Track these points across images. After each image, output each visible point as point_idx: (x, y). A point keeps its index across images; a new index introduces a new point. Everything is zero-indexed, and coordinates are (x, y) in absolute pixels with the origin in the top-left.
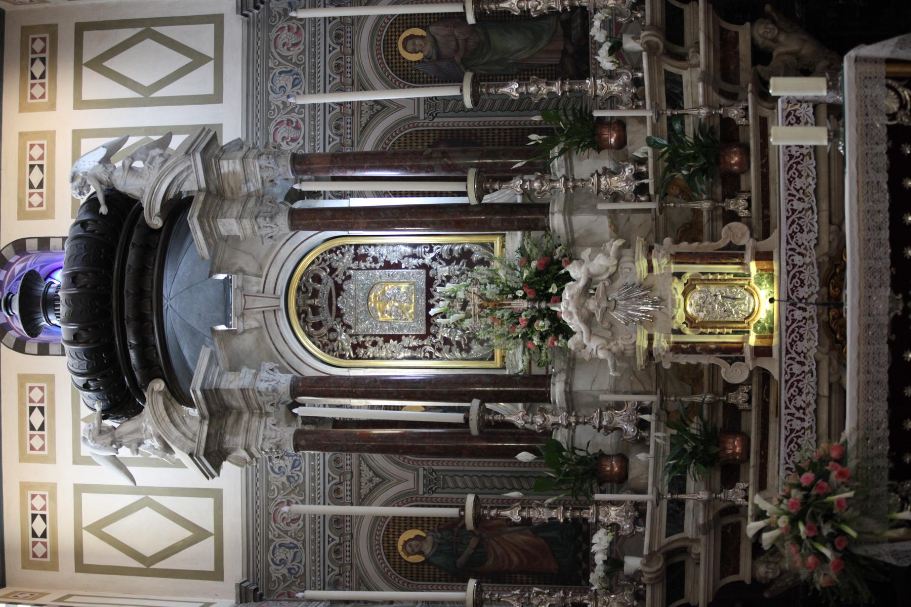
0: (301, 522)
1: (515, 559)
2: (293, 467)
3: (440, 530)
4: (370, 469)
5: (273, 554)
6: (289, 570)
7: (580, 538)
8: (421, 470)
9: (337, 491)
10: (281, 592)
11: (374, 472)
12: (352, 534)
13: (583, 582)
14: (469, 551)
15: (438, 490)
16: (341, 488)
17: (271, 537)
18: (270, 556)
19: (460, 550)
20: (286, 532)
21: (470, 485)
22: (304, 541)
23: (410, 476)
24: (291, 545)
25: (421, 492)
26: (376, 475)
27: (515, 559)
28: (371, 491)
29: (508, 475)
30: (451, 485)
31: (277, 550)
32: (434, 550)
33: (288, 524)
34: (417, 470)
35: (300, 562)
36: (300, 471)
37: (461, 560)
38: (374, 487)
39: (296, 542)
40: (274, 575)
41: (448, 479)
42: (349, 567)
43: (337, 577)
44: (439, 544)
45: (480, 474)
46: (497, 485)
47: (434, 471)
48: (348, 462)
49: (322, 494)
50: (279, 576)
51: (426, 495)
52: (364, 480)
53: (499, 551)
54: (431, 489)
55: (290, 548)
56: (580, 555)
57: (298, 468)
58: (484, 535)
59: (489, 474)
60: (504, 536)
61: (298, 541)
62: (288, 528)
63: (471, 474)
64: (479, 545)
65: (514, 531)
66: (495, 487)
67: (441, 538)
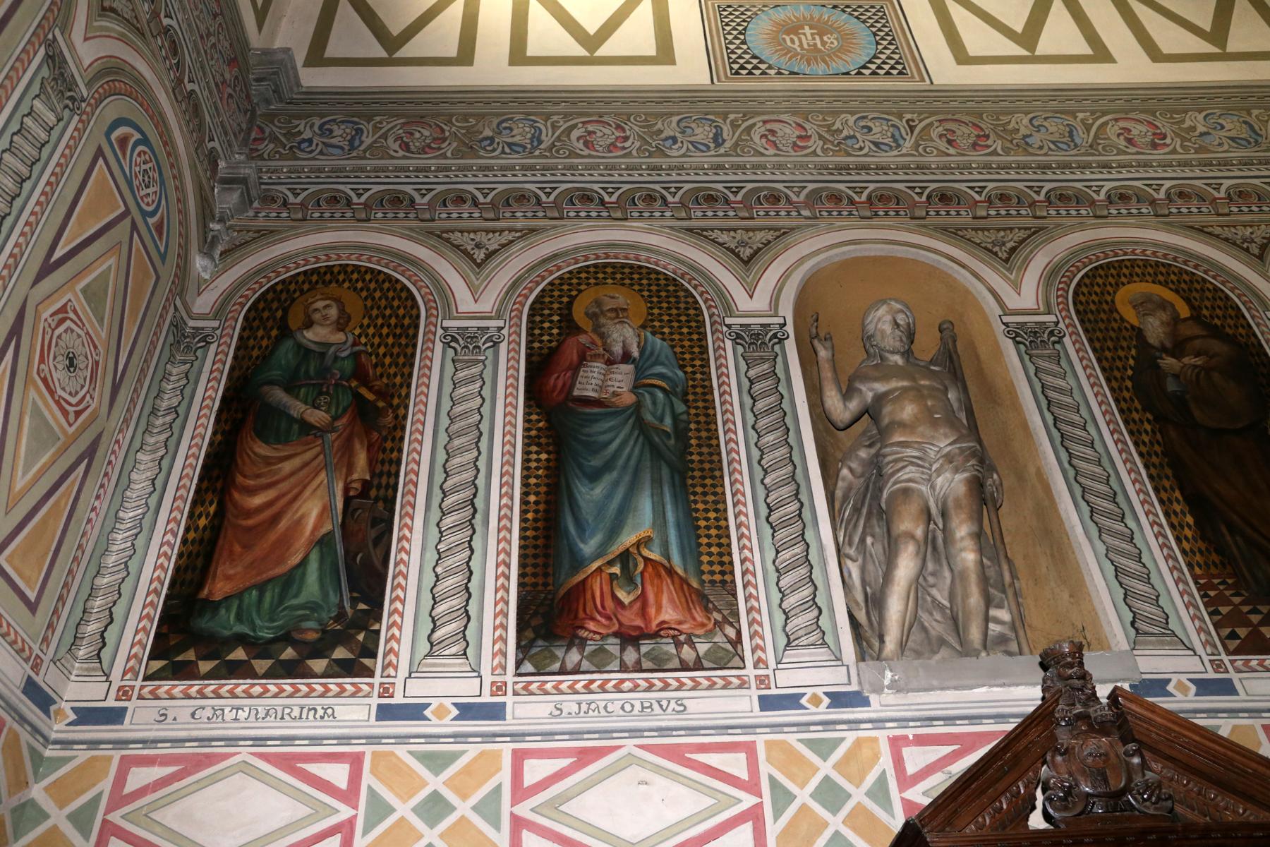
0: (401, 153)
1: (258, 500)
2: (510, 145)
3: (356, 356)
4: (503, 246)
5: (343, 122)
6: (310, 141)
7: (289, 653)
8: (500, 323)
9: (460, 200)
10: (267, 131)
11: (496, 251)
12: (368, 220)
13: (157, 665)
14: (297, 408)
15: (450, 352)
16: (466, 206)
17: (378, 119)
18: (340, 118)
19: (303, 390)
20: (385, 136)
21: (458, 409)
22: (364, 158)
23: (488, 303)
24: (357, 143)
25: (447, 323)
26: (489, 255)
27: (258, 500)
28: (458, 247)
29: (481, 482)
30: (461, 375)
31: (350, 125)
32: (313, 347)
33: (399, 138)
34: (498, 317)
35: (321, 153)
36: (503, 152)
37: (279, 395)
38: (465, 252)
39: (362, 148)
40: (303, 122)
41: (476, 370)
42: (300, 216)
43: (280, 201)
44: (323, 355)
45: (484, 427)
46: (456, 461)
47: (496, 344)
48: (518, 214)
49: (455, 180)
50: (301, 128)
51: (440, 332)
52: (481, 237)
53: (287, 467)
54: (454, 339)
55: (351, 142)
56: (239, 654)
57: (507, 150)
58: (331, 437)
59: (483, 445)
60: (323, 475)
61: (365, 151)
62: (390, 140)
63: (486, 410)
64: (306, 427)
65: (331, 494)
66: (449, 456)
67: (336, 358)
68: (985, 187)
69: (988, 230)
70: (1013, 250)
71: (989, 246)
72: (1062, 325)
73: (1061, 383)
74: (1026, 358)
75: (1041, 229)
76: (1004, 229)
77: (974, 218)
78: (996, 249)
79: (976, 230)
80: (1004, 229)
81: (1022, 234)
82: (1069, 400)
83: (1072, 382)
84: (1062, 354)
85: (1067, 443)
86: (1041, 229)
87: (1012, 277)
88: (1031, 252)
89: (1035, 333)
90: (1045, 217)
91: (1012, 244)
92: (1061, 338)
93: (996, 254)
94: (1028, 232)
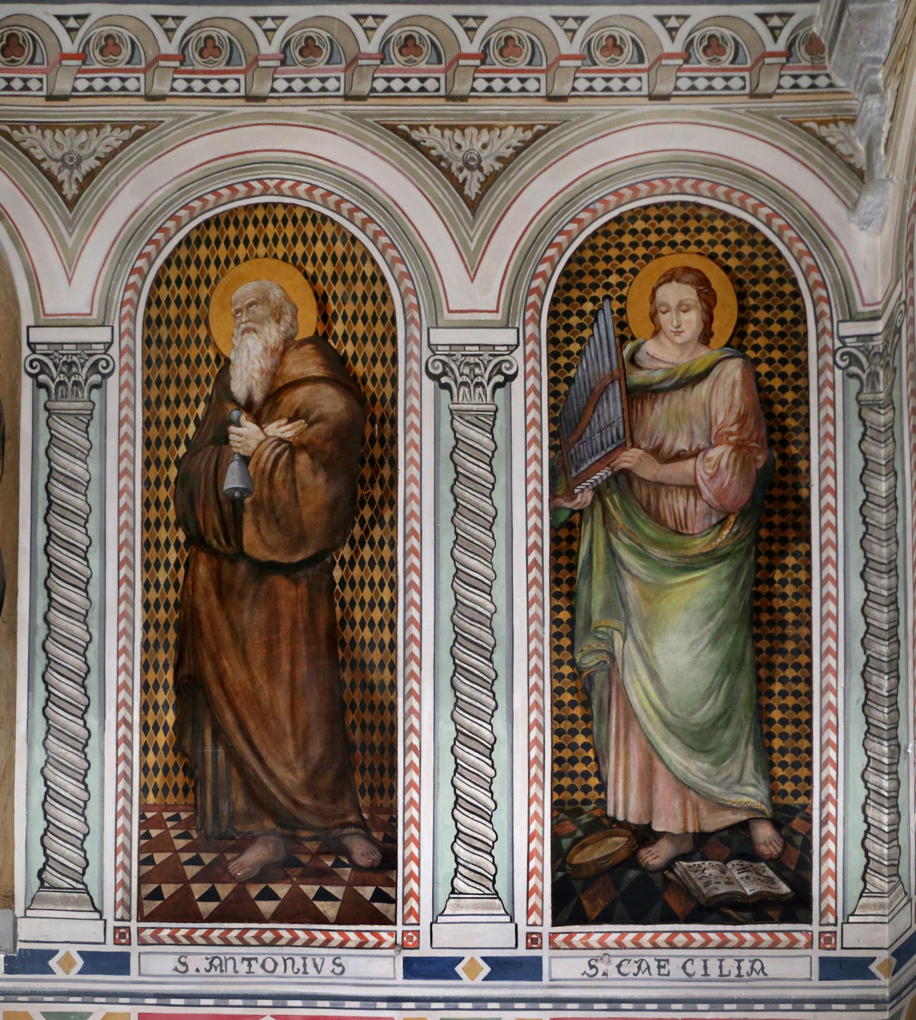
68: (84, 17)
69: (62, 127)
70: (91, 176)
71: (54, 167)
72: (114, 351)
73: (78, 468)
74: (43, 415)
75: (149, 126)
76: (88, 127)
77: (49, 98)
78: (63, 176)
79: (42, 126)
80: (88, 127)
81: (114, 138)
82: (79, 502)
83: (94, 468)
84: (96, 413)
85: (54, 582)
86: (149, 126)
87: (70, 242)
88: (117, 182)
89: (71, 364)
90: (163, 97)
91: (90, 164)
92: (105, 376)
93: (59, 186)
94: (126, 135)
